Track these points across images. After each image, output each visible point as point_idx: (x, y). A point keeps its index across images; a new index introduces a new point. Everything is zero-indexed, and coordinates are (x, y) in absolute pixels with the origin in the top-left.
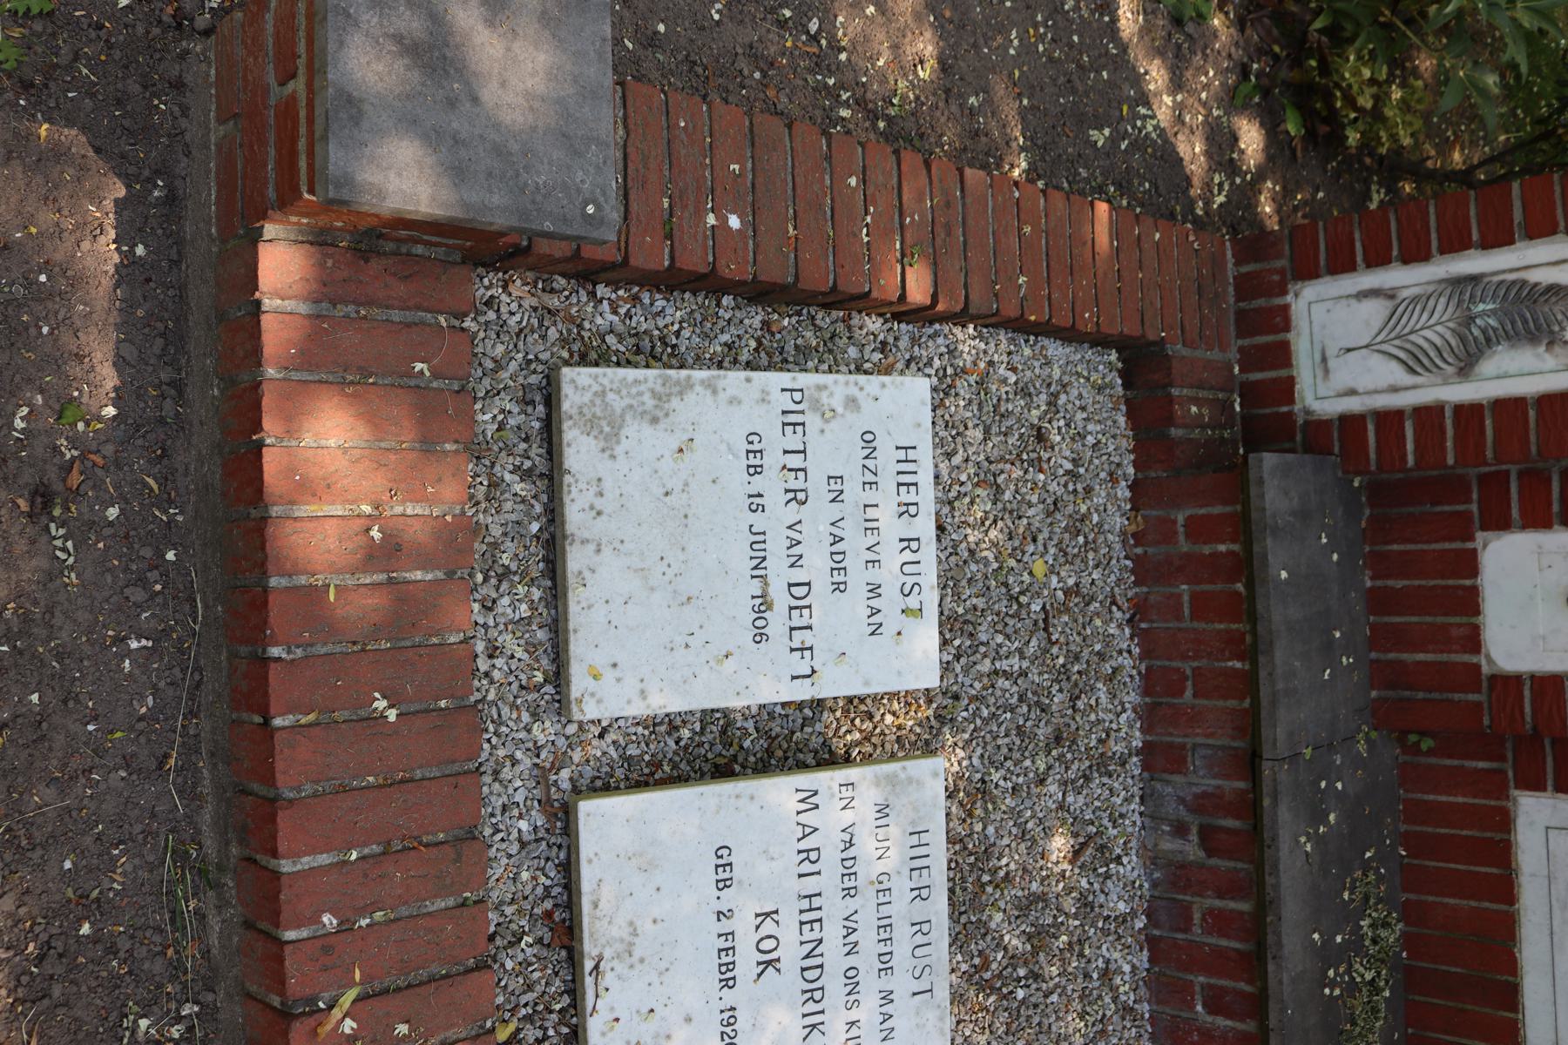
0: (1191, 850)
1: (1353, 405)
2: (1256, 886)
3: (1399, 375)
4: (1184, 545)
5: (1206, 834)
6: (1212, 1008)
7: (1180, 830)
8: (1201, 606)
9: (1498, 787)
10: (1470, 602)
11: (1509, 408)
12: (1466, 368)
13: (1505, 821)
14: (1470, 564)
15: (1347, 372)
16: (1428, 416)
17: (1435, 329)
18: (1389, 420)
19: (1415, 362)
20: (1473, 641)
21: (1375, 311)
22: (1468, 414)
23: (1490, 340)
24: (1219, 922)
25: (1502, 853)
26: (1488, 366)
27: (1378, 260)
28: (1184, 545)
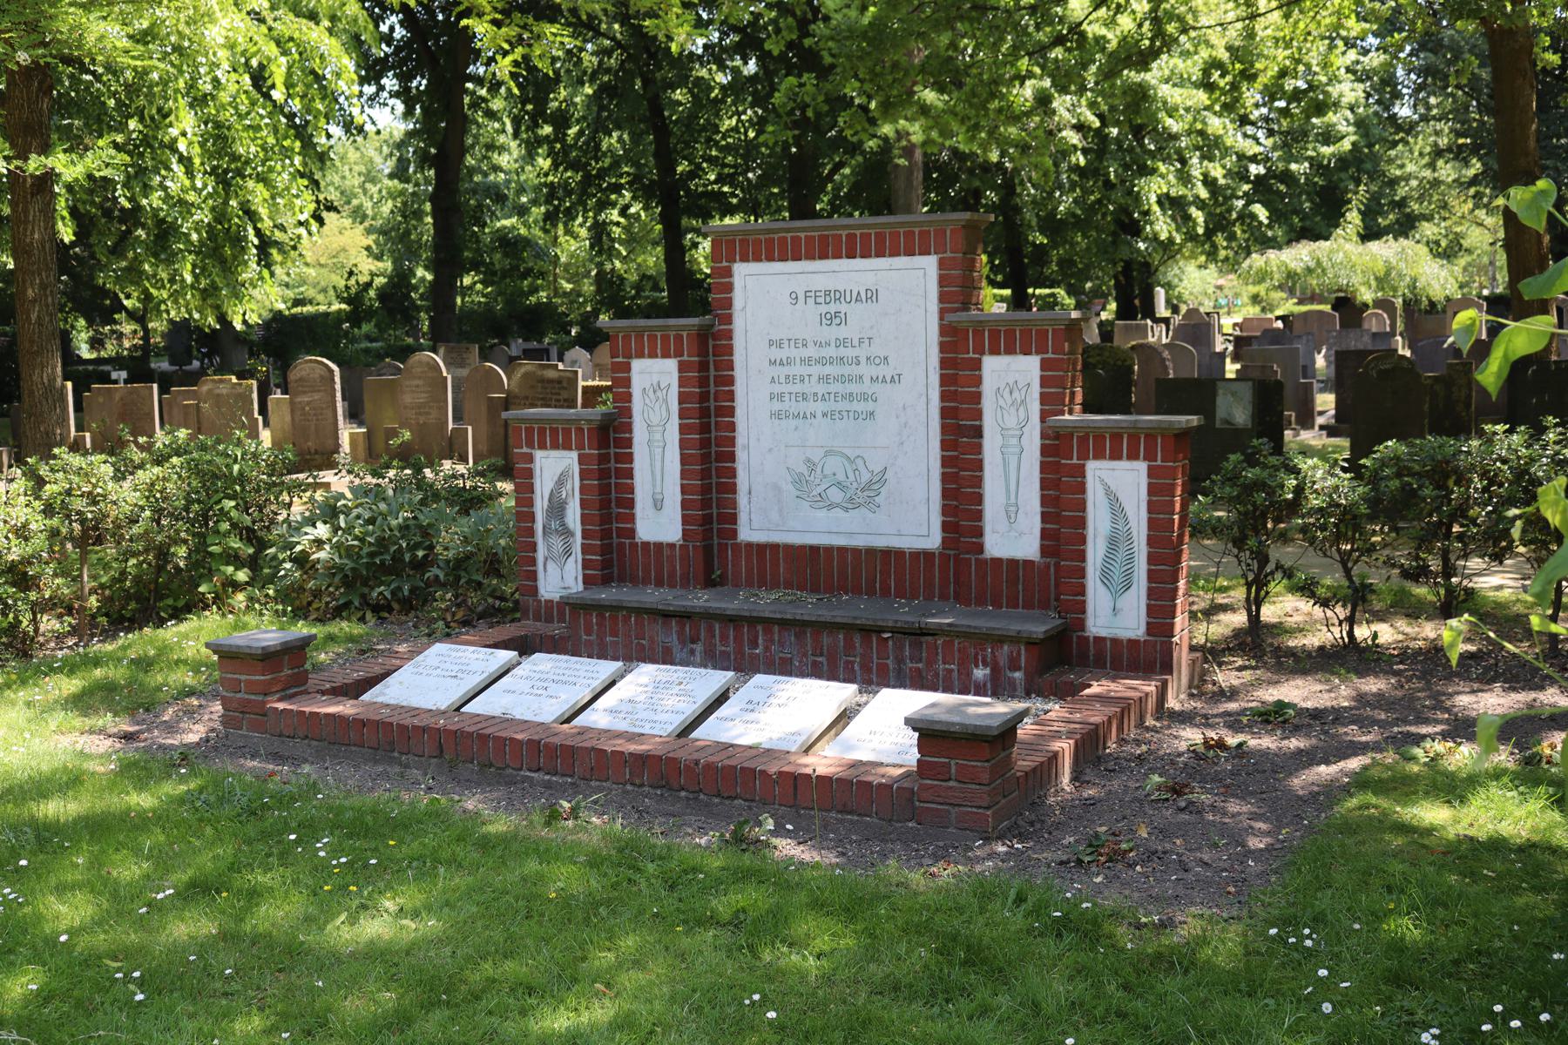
0: (699, 648)
1: (580, 578)
2: (709, 616)
3: (572, 559)
4: (593, 637)
5: (693, 641)
6: (756, 646)
7: (692, 652)
8: (614, 633)
9: (737, 547)
10: (659, 546)
11: (585, 519)
12: (572, 534)
13: (749, 545)
14: (646, 545)
15: (570, 581)
16: (585, 549)
17: (558, 543)
18: (586, 564)
19: (568, 553)
20: (672, 546)
21: (551, 566)
22: (586, 534)
23: (563, 524)
24: (724, 638)
25: (762, 548)
26: (571, 525)
27: (533, 562)
28: (593, 637)
